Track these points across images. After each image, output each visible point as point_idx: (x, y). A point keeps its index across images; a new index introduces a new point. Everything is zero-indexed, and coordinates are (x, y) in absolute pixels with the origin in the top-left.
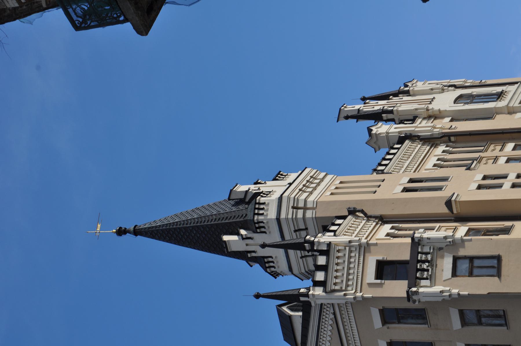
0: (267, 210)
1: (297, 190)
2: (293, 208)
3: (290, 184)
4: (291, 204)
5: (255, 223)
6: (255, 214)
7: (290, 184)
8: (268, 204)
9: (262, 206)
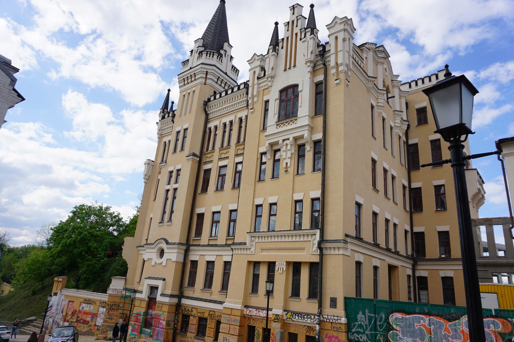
0: (209, 59)
2: (207, 72)
3: (226, 74)
4: (209, 71)
5: (202, 53)
6: (207, 52)
7: (226, 74)
8: (212, 59)
9: (211, 56)
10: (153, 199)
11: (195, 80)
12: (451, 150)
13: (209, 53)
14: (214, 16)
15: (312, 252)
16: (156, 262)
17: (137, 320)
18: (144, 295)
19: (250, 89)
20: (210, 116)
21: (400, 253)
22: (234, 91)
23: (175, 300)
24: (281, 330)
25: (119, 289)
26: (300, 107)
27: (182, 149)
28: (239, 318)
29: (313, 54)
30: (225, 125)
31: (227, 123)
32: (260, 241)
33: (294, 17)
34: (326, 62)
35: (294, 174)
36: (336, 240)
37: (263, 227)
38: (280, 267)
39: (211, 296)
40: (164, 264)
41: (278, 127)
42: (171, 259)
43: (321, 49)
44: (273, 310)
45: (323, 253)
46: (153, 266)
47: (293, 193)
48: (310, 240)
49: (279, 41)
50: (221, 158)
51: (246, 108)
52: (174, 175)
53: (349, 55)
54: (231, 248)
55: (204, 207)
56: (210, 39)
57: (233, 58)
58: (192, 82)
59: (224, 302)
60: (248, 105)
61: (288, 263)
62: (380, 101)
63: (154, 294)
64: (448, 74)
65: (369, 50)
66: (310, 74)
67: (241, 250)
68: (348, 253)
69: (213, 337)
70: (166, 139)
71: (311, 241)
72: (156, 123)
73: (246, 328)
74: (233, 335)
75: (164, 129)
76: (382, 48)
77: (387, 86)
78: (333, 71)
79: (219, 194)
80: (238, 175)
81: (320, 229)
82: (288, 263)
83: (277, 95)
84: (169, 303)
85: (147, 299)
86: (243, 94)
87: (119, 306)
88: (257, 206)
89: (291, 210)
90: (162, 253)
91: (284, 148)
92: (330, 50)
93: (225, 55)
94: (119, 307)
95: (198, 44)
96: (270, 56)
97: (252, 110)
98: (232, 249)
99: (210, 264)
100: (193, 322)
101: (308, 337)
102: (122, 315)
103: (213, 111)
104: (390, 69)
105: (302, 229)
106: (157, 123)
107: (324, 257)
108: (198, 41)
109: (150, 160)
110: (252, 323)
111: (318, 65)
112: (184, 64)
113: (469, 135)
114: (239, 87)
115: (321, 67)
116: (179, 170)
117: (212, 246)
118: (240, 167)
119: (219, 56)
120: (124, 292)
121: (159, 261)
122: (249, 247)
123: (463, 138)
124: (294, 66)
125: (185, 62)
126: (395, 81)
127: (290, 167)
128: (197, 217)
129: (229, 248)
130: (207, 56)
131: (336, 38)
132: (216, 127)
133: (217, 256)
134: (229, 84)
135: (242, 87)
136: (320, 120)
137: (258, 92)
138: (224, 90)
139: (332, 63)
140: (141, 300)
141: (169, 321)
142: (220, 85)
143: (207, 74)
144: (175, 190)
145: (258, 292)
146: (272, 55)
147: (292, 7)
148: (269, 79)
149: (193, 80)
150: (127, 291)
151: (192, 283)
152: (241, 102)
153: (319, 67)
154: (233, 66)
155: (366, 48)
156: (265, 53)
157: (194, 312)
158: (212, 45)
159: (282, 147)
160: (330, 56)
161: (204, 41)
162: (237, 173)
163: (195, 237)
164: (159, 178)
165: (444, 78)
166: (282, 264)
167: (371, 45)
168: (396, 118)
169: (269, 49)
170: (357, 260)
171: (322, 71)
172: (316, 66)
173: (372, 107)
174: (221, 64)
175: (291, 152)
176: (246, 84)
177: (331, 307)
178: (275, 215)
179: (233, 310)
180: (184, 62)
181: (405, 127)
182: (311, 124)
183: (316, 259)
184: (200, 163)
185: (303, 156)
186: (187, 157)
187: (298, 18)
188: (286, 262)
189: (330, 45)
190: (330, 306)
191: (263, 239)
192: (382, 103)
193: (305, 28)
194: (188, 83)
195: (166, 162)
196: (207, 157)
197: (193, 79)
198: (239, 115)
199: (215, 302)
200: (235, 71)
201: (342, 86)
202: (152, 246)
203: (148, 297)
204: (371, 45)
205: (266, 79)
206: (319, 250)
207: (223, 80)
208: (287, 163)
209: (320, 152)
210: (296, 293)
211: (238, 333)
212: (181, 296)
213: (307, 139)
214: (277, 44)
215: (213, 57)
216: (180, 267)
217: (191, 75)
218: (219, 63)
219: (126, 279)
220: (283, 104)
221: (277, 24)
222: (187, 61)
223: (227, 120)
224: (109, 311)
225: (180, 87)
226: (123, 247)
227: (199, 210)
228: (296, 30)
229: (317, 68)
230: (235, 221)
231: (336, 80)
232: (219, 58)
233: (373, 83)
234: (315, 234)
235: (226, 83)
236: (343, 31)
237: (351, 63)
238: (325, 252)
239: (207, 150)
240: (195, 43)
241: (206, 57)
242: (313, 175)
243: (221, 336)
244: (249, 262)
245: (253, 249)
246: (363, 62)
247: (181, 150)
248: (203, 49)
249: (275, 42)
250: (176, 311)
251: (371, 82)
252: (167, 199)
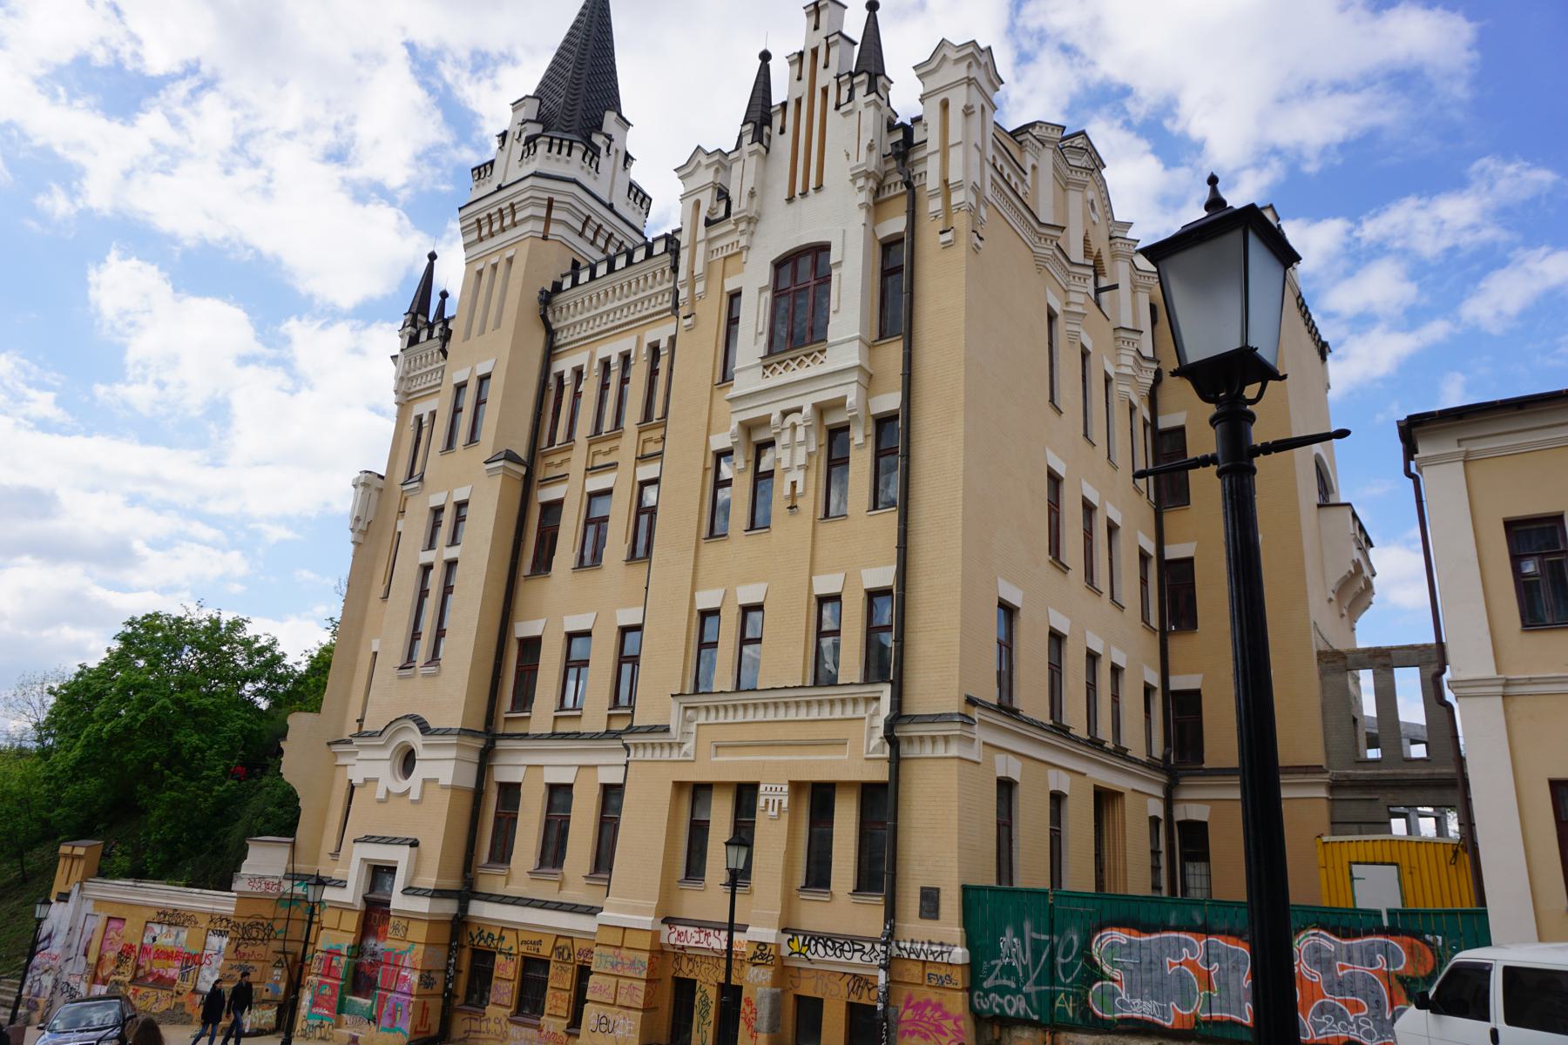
0: (558, 160)
1: (587, 213)
2: (551, 201)
3: (610, 207)
4: (556, 198)
6: (552, 138)
7: (610, 207)
8: (568, 162)
9: (565, 151)
10: (381, 593)
11: (514, 224)
12: (1217, 427)
13: (558, 142)
14: (573, 27)
15: (868, 753)
16: (391, 790)
17: (328, 971)
18: (351, 894)
19: (684, 256)
20: (562, 338)
21: (1129, 753)
22: (636, 260)
23: (449, 907)
24: (774, 990)
25: (273, 877)
26: (835, 312)
27: (473, 438)
28: (645, 957)
29: (874, 153)
30: (606, 364)
31: (614, 360)
32: (712, 719)
33: (818, 39)
34: (915, 177)
35: (814, 516)
36: (940, 715)
37: (722, 678)
38: (773, 799)
39: (560, 889)
40: (414, 795)
41: (768, 373)
42: (436, 780)
43: (899, 136)
44: (749, 929)
45: (902, 755)
46: (380, 801)
47: (811, 574)
48: (864, 715)
49: (772, 110)
50: (593, 468)
51: (673, 314)
52: (447, 518)
53: (983, 158)
54: (624, 744)
55: (541, 618)
56: (562, 100)
57: (633, 159)
58: (503, 230)
59: (601, 910)
60: (676, 306)
61: (796, 787)
62: (1073, 297)
63: (383, 887)
64: (1215, 203)
65: (1044, 145)
66: (864, 211)
67: (653, 748)
68: (974, 753)
69: (566, 1018)
70: (422, 408)
71: (864, 718)
72: (392, 357)
73: (667, 989)
74: (628, 1008)
75: (416, 377)
76: (1080, 141)
77: (1095, 254)
78: (935, 205)
79: (588, 576)
80: (644, 519)
81: (891, 682)
82: (796, 787)
83: (765, 276)
84: (429, 914)
85: (359, 905)
86: (663, 272)
87: (272, 929)
88: (705, 614)
89: (807, 627)
90: (408, 761)
91: (785, 438)
92: (926, 141)
93: (608, 150)
94: (273, 933)
95: (521, 115)
96: (746, 156)
97: (688, 321)
98: (627, 747)
99: (559, 794)
100: (506, 971)
101: (852, 1008)
102: (282, 956)
103: (571, 321)
104: (1106, 202)
105: (839, 682)
106: (394, 358)
107: (903, 766)
108: (524, 105)
109: (370, 472)
110: (686, 971)
111: (890, 186)
112: (480, 173)
113: (1271, 384)
114: (649, 248)
115: (899, 191)
116: (461, 505)
117: (565, 736)
118: (650, 496)
119: (590, 153)
120: (287, 886)
121: (400, 785)
122: (678, 741)
123: (1251, 391)
124: (819, 188)
125: (482, 169)
127: (803, 495)
128: (519, 650)
129: (617, 744)
130: (550, 151)
131: (945, 105)
132: (578, 373)
133: (581, 769)
134: (621, 238)
135: (659, 248)
136: (893, 352)
137: (709, 265)
138: (603, 256)
139: (932, 182)
140: (342, 908)
141: (429, 971)
142: (593, 243)
143: (550, 207)
144: (451, 564)
145: (704, 875)
146: (751, 154)
147: (812, 7)
148: (742, 226)
149: (508, 226)
150: (296, 883)
151: (502, 853)
152: (656, 295)
153: (892, 193)
154: (631, 185)
155: (1035, 137)
156: (729, 146)
157: (509, 942)
158: (568, 119)
159: (779, 433)
160: (924, 159)
161: (541, 103)
162: (644, 513)
163: (513, 710)
164: (399, 530)
165: (1205, 214)
166: (779, 789)
167: (1049, 130)
168: (1123, 351)
169: (741, 133)
170: (1001, 773)
171: (903, 203)
172: (884, 188)
173: (1052, 316)
174: (595, 178)
175: (807, 448)
176: (671, 241)
177: (921, 916)
178: (758, 641)
179: (627, 931)
180: (479, 168)
181: (1148, 379)
182: (866, 366)
183: (880, 774)
184: (528, 483)
185: (845, 461)
186: (486, 462)
187: (830, 40)
188: (791, 783)
189: (926, 125)
190: (921, 913)
191: (722, 714)
192: (1082, 304)
193: (850, 73)
194: (492, 235)
195: (421, 479)
196: (551, 464)
197: (507, 221)
198: (651, 335)
199: (573, 909)
200: (638, 201)
201: (961, 252)
202: (378, 739)
203: (365, 898)
204: (1049, 130)
205: (732, 227)
206: (887, 747)
207: (600, 227)
208: (794, 484)
209: (894, 450)
210: (818, 876)
211: (641, 1002)
212: (467, 892)
213: (855, 410)
214: (767, 120)
215: (569, 154)
216: (466, 803)
217: (501, 211)
218: (589, 173)
219: (293, 844)
220: (784, 303)
221: (765, 56)
222: (488, 166)
223: (612, 349)
224: (238, 946)
225: (466, 246)
226: (283, 745)
227: (524, 628)
228: (825, 78)
229: (887, 195)
230: (635, 660)
231: (942, 233)
232: (587, 160)
233: (1054, 244)
234: (878, 699)
235: (611, 235)
236: (965, 86)
237: (988, 182)
238: (905, 751)
239: (552, 441)
240: (514, 110)
241: (549, 154)
242: (871, 518)
243: (590, 1012)
244: (679, 786)
245: (689, 746)
246: (1023, 181)
247: (470, 443)
248: (537, 129)
249: (760, 114)
250: (451, 941)
251: (1049, 241)
252: (423, 593)
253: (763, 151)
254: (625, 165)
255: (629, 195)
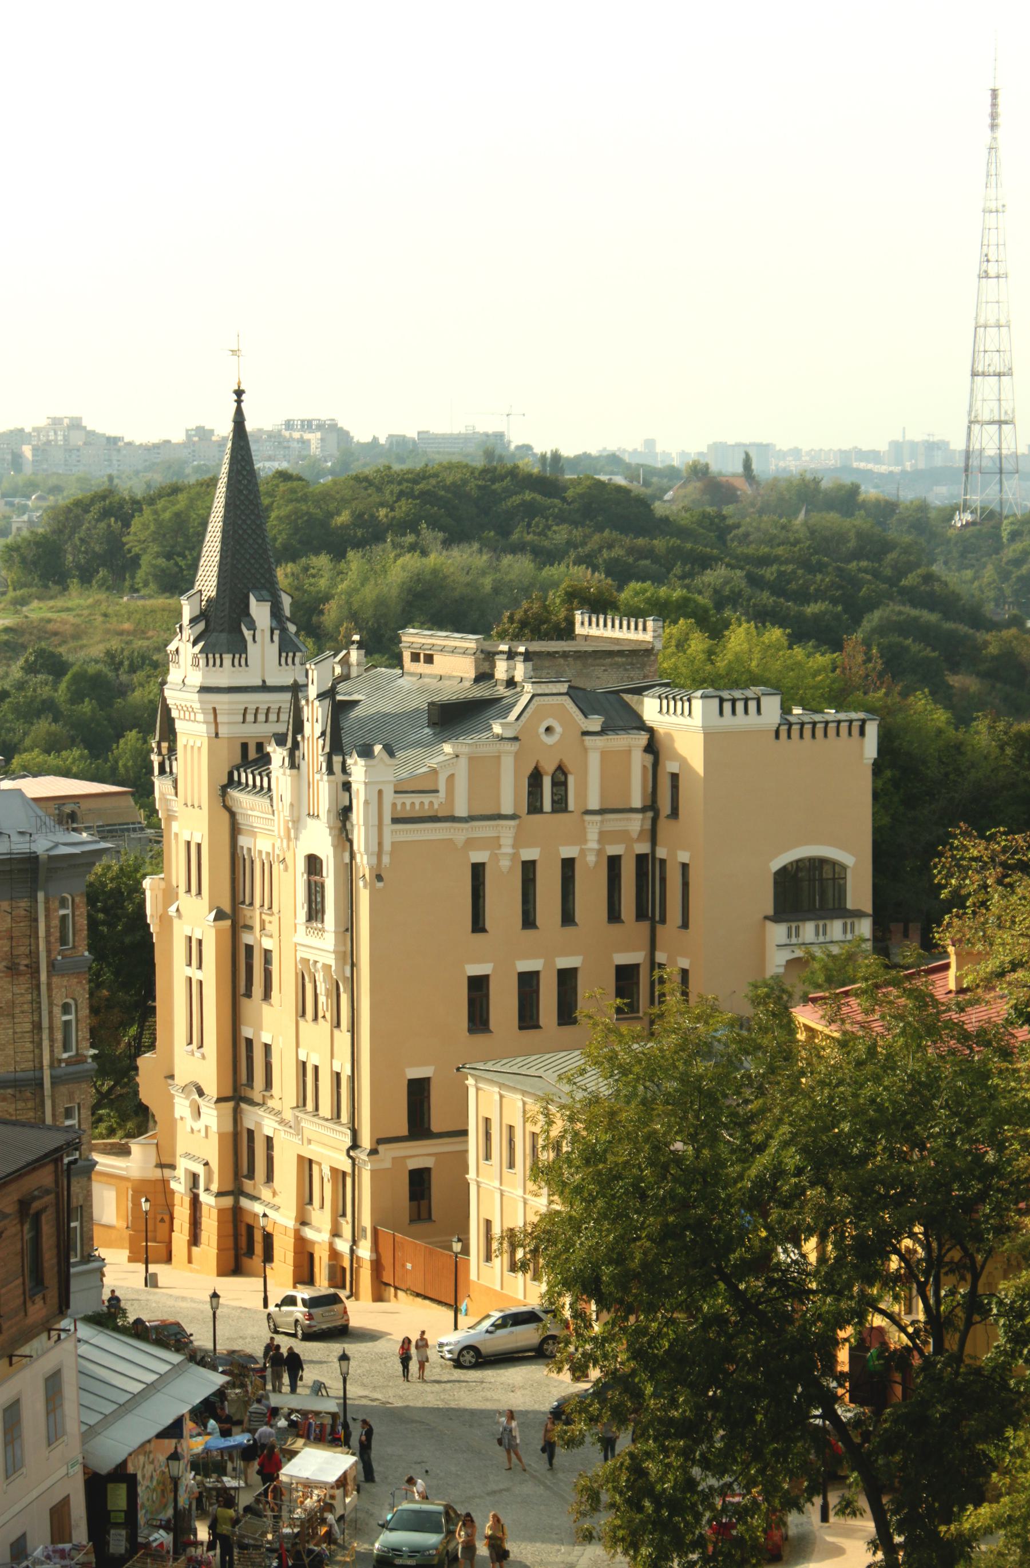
2: (214, 709)
3: (264, 688)
20: (240, 819)
23: (228, 1202)
61: (334, 1170)
62: (503, 841)
68: (387, 1164)
82: (334, 1170)
100: (258, 1237)
119: (237, 656)
126: (587, 738)
142: (255, 722)
181: (636, 823)
216: (230, 1141)
244: (300, 1158)
248: (201, 626)
253: (295, 771)
254: (272, 640)
255: (280, 664)
